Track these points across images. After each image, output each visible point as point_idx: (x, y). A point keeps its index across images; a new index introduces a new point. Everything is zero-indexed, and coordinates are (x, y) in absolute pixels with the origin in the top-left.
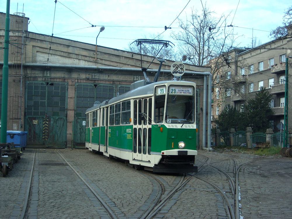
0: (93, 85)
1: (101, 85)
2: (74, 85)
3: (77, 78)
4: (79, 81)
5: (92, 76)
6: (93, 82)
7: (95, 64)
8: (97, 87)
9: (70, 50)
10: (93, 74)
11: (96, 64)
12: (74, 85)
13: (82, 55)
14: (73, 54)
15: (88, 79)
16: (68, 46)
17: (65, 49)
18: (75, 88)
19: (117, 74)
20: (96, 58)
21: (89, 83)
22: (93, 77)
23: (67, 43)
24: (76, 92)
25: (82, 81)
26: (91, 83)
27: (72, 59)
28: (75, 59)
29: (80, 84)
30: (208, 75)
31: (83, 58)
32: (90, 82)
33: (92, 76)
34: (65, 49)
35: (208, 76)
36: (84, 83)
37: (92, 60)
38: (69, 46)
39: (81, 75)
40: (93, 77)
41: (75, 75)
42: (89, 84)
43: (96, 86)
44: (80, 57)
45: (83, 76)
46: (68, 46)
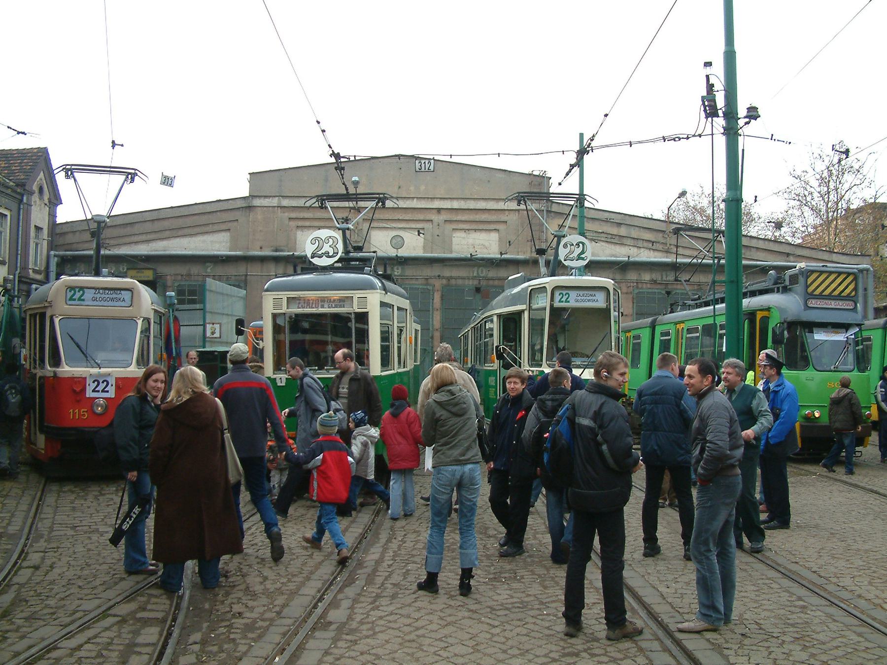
0: (664, 292)
1: (678, 291)
2: (631, 293)
3: (637, 280)
4: (640, 286)
5: (662, 275)
6: (663, 287)
7: (665, 254)
8: (670, 296)
9: (623, 231)
10: (664, 273)
11: (669, 254)
12: (631, 293)
13: (643, 240)
14: (628, 237)
15: (654, 282)
16: (619, 225)
17: (614, 231)
18: (633, 298)
19: (706, 271)
20: (668, 245)
21: (657, 289)
22: (664, 278)
23: (618, 219)
24: (635, 304)
25: (644, 286)
26: (661, 289)
27: (627, 247)
28: (631, 247)
29: (641, 291)
30: (867, 270)
31: (645, 244)
32: (659, 286)
33: (662, 275)
34: (614, 231)
35: (865, 272)
36: (646, 288)
37: (660, 247)
38: (621, 224)
39: (642, 275)
40: (664, 278)
41: (632, 276)
42: (656, 291)
43: (668, 293)
44: (640, 244)
45: (647, 277)
46: (619, 225)
